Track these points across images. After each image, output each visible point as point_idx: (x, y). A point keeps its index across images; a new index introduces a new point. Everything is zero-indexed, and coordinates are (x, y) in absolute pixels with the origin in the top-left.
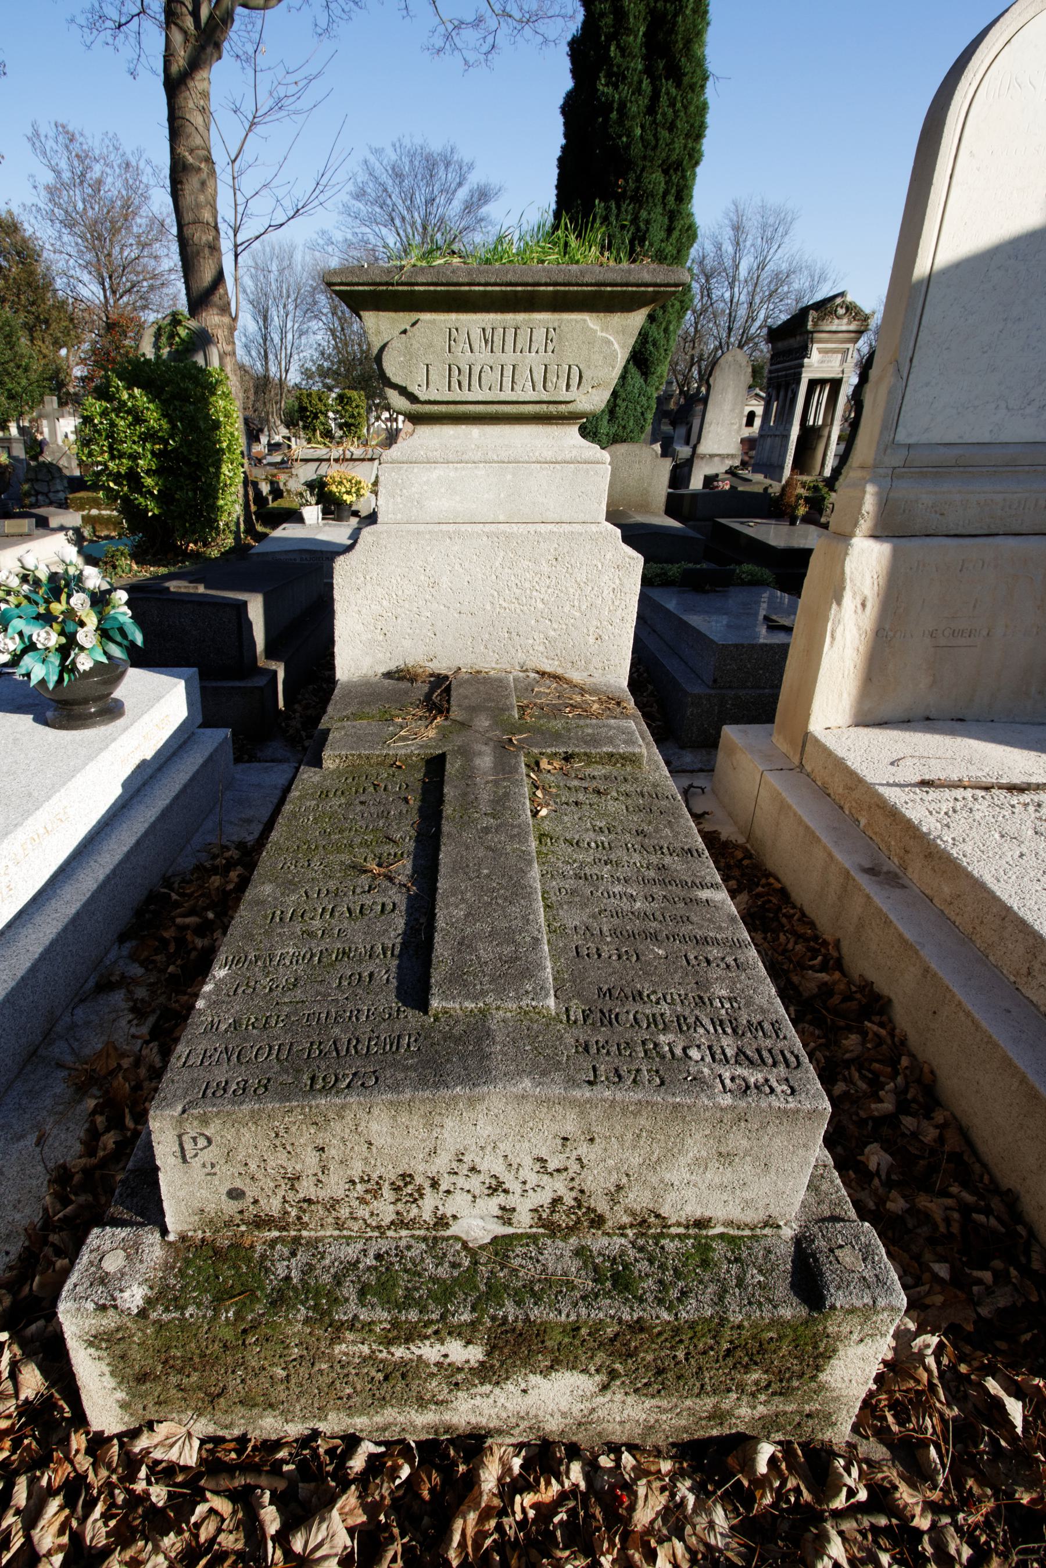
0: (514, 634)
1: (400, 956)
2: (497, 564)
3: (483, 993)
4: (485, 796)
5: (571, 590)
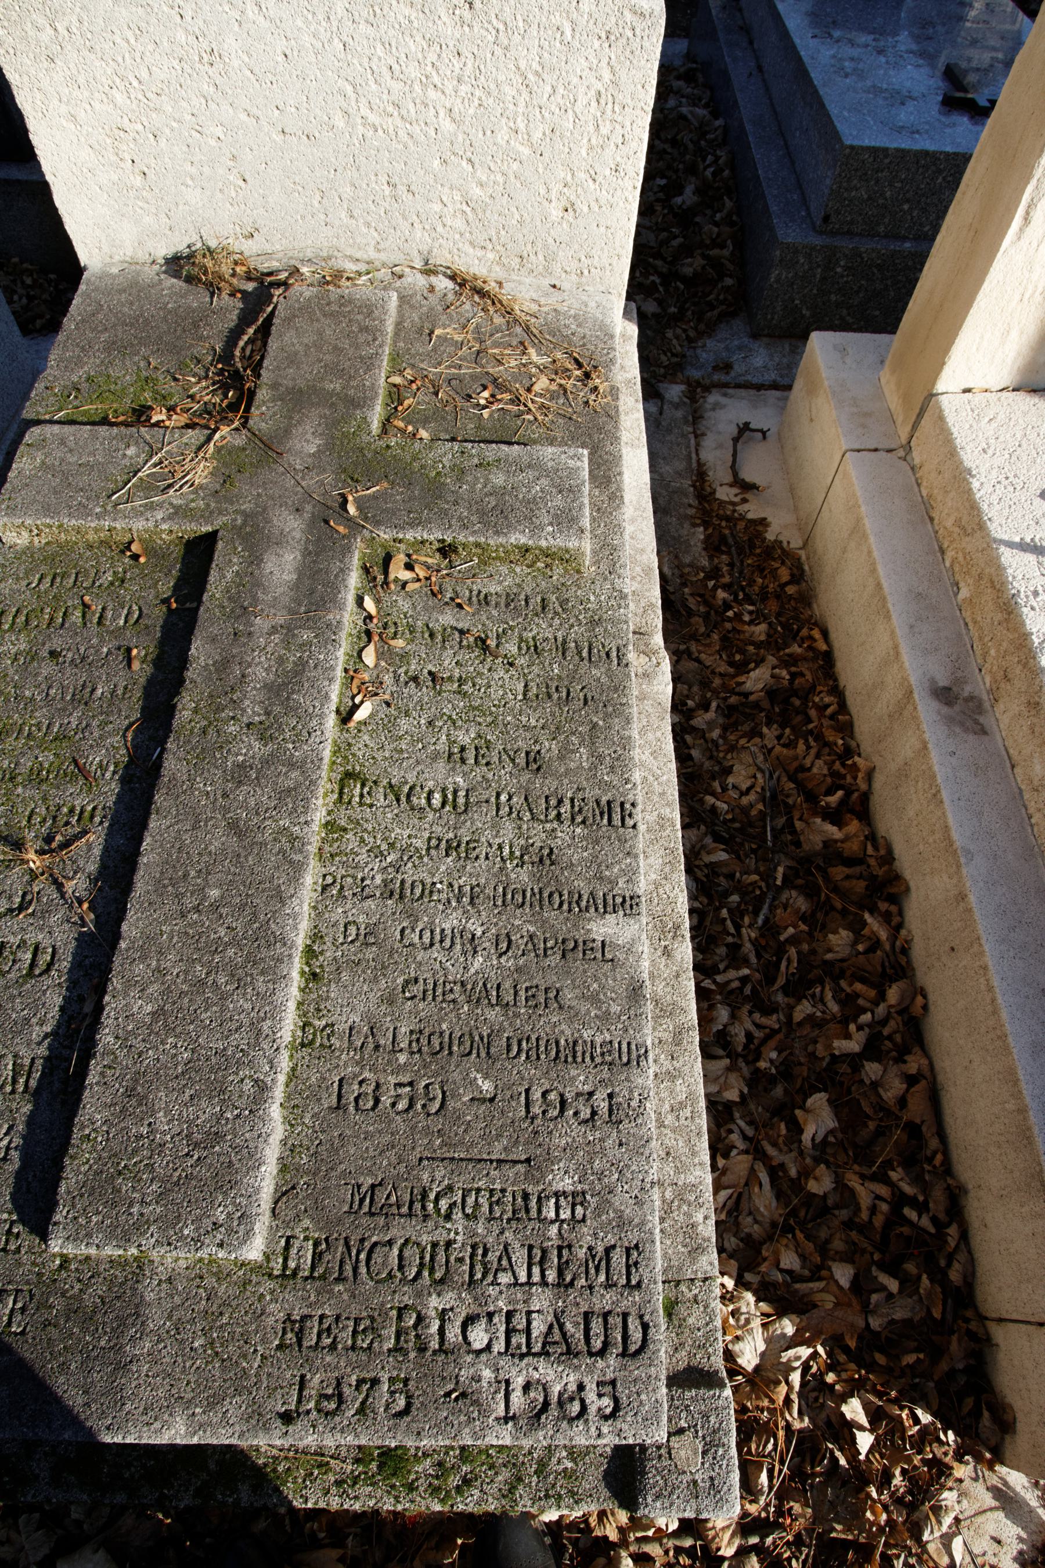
0: (402, 189)
1: (37, 1094)
2: (340, 11)
3: (141, 1226)
4: (260, 672)
5: (509, 91)
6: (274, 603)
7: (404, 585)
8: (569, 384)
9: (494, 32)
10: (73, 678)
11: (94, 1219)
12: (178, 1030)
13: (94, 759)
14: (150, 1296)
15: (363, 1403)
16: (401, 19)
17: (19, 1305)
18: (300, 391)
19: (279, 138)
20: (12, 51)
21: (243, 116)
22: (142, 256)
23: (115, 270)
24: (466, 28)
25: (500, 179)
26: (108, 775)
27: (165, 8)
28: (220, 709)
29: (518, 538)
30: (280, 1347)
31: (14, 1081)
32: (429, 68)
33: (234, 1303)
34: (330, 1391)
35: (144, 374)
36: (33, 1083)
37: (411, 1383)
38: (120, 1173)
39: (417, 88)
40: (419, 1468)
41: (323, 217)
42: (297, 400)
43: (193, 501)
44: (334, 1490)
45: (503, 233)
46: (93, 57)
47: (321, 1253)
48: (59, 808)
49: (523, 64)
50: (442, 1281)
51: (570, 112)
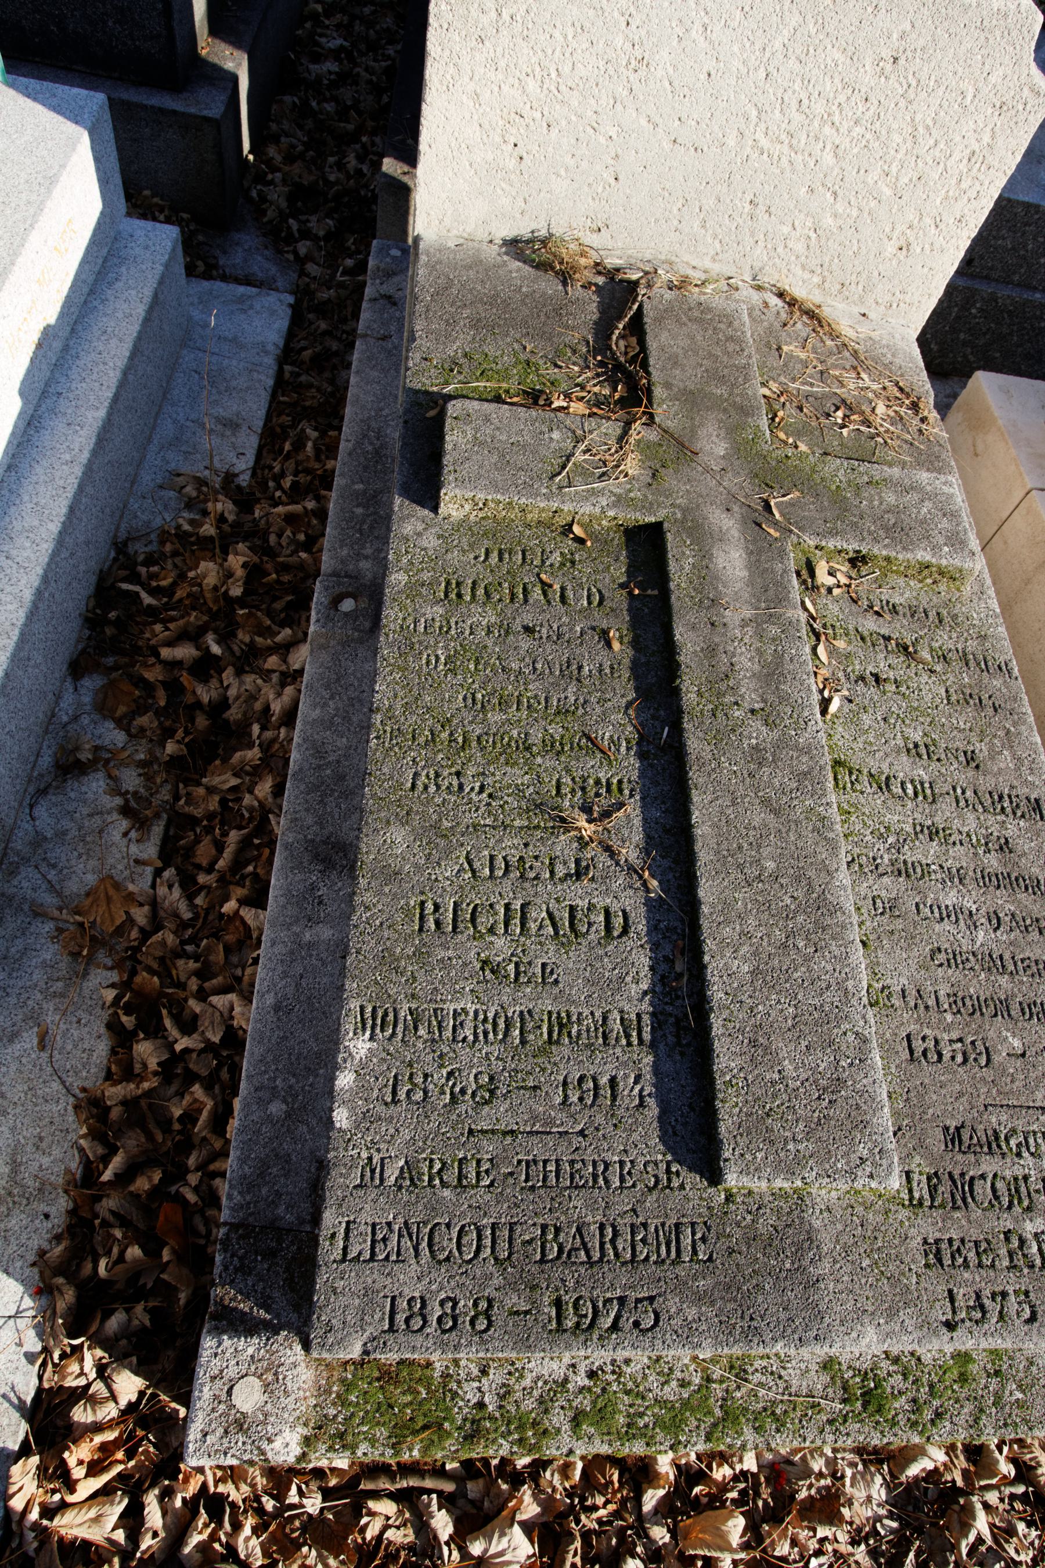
0: (762, 208)
1: (653, 1045)
2: (778, 45)
3: (800, 1160)
4: (746, 662)
5: (897, 138)
6: (737, 597)
7: (830, 590)
8: (903, 411)
9: (905, 86)
10: (556, 654)
11: (759, 1155)
12: (777, 987)
13: (605, 734)
14: (817, 1224)
15: (1001, 1312)
16: (829, 61)
17: (699, 1235)
18: (692, 392)
19: (667, 145)
20: (445, 26)
21: (643, 122)
22: (482, 235)
23: (451, 244)
24: (883, 79)
25: (855, 213)
26: (623, 749)
27: (616, 14)
28: (720, 695)
29: (923, 555)
30: (927, 1266)
31: (628, 1036)
32: (834, 108)
33: (883, 1229)
34: (972, 1303)
35: (522, 357)
36: (647, 1036)
37: (1031, 1294)
38: (768, 1115)
39: (816, 124)
40: (897, 1405)
41: (676, 223)
42: (692, 400)
43: (630, 491)
44: (828, 1428)
45: (836, 261)
46: (524, 44)
47: (935, 1186)
48: (584, 779)
49: (919, 117)
50: (1029, 1209)
51: (942, 165)
